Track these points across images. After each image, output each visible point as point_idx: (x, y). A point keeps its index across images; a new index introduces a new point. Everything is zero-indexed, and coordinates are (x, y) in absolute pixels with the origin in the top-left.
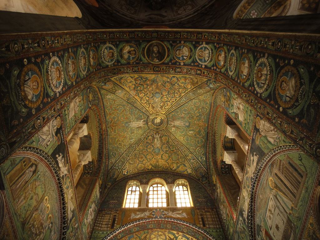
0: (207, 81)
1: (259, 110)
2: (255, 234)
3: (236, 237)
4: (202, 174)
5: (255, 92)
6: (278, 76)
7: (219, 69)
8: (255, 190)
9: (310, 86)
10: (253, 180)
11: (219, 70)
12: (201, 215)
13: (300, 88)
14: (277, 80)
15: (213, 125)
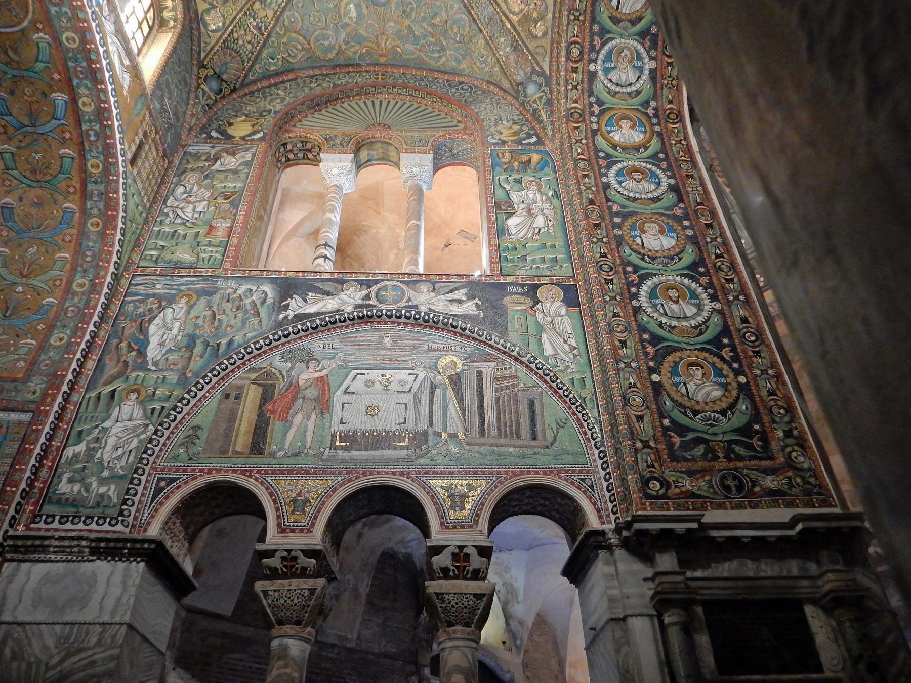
0: (542, 74)
1: (611, 314)
2: (277, 347)
3: (193, 283)
4: (225, 72)
5: (634, 290)
6: (702, 350)
7: (598, 123)
8: (388, 320)
9: (731, 431)
10: (413, 313)
11: (595, 126)
12: (145, 134)
13: (717, 412)
14: (695, 350)
15: (394, 87)
